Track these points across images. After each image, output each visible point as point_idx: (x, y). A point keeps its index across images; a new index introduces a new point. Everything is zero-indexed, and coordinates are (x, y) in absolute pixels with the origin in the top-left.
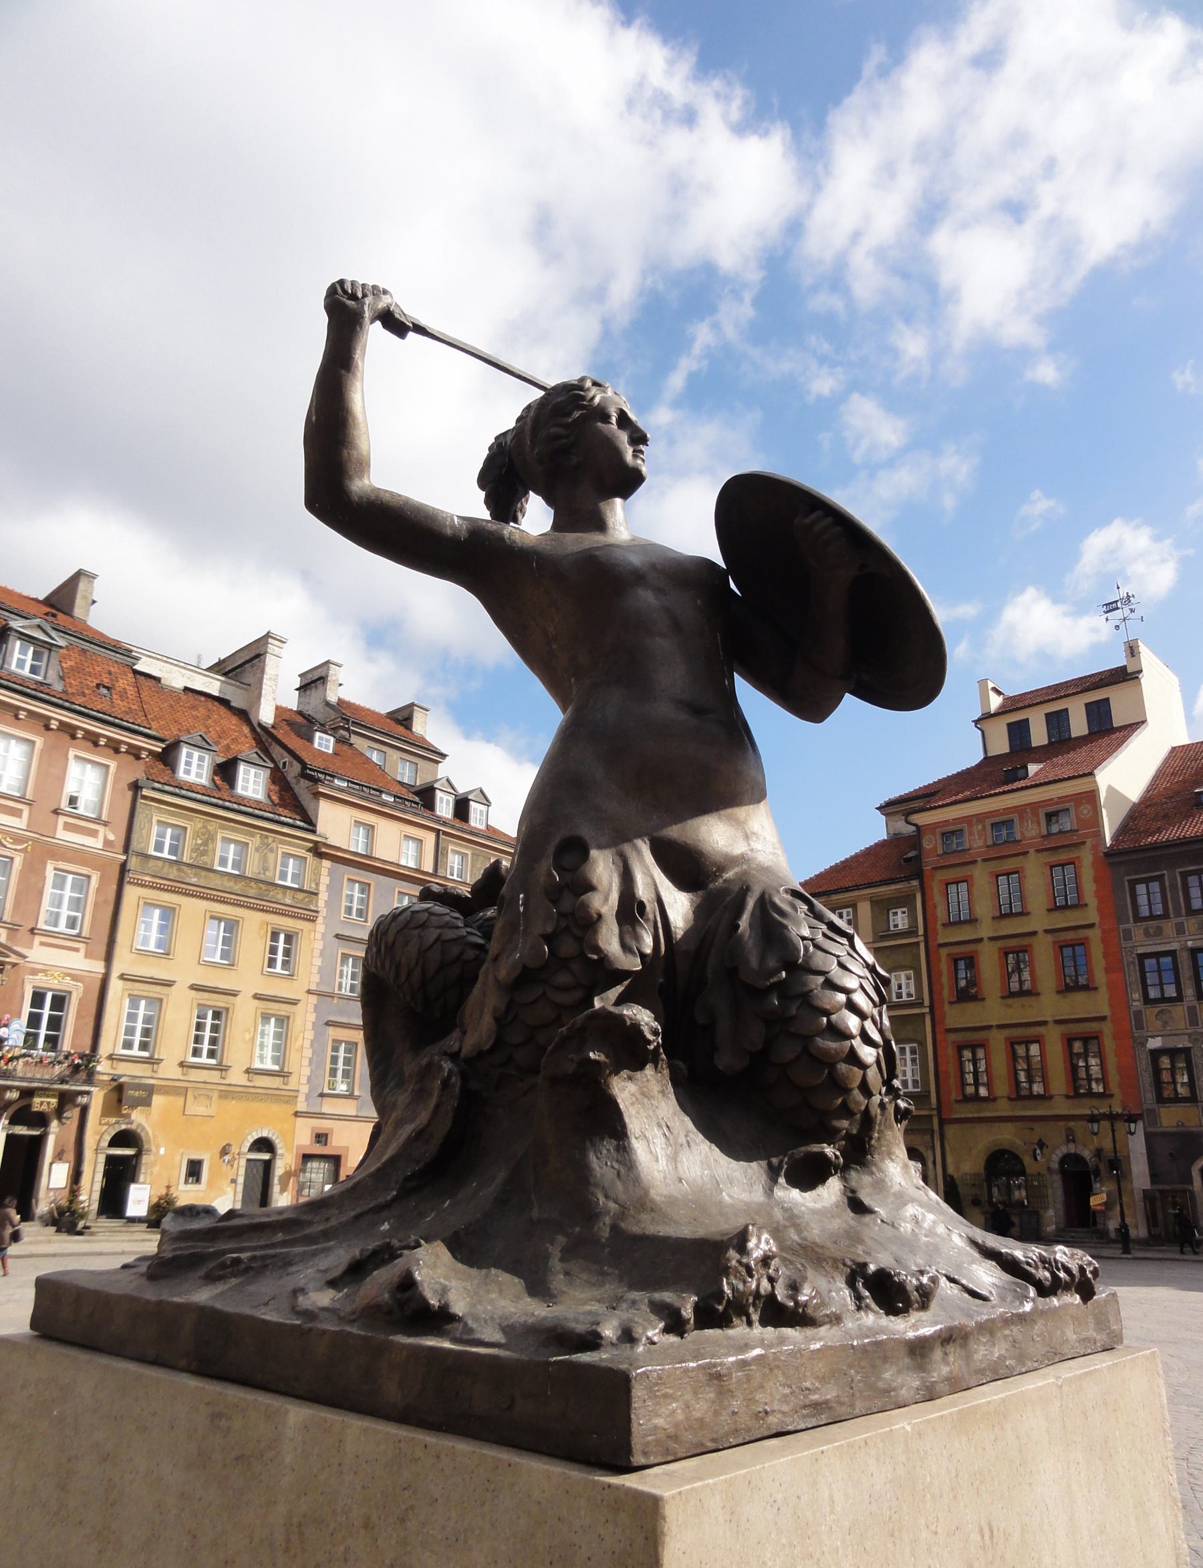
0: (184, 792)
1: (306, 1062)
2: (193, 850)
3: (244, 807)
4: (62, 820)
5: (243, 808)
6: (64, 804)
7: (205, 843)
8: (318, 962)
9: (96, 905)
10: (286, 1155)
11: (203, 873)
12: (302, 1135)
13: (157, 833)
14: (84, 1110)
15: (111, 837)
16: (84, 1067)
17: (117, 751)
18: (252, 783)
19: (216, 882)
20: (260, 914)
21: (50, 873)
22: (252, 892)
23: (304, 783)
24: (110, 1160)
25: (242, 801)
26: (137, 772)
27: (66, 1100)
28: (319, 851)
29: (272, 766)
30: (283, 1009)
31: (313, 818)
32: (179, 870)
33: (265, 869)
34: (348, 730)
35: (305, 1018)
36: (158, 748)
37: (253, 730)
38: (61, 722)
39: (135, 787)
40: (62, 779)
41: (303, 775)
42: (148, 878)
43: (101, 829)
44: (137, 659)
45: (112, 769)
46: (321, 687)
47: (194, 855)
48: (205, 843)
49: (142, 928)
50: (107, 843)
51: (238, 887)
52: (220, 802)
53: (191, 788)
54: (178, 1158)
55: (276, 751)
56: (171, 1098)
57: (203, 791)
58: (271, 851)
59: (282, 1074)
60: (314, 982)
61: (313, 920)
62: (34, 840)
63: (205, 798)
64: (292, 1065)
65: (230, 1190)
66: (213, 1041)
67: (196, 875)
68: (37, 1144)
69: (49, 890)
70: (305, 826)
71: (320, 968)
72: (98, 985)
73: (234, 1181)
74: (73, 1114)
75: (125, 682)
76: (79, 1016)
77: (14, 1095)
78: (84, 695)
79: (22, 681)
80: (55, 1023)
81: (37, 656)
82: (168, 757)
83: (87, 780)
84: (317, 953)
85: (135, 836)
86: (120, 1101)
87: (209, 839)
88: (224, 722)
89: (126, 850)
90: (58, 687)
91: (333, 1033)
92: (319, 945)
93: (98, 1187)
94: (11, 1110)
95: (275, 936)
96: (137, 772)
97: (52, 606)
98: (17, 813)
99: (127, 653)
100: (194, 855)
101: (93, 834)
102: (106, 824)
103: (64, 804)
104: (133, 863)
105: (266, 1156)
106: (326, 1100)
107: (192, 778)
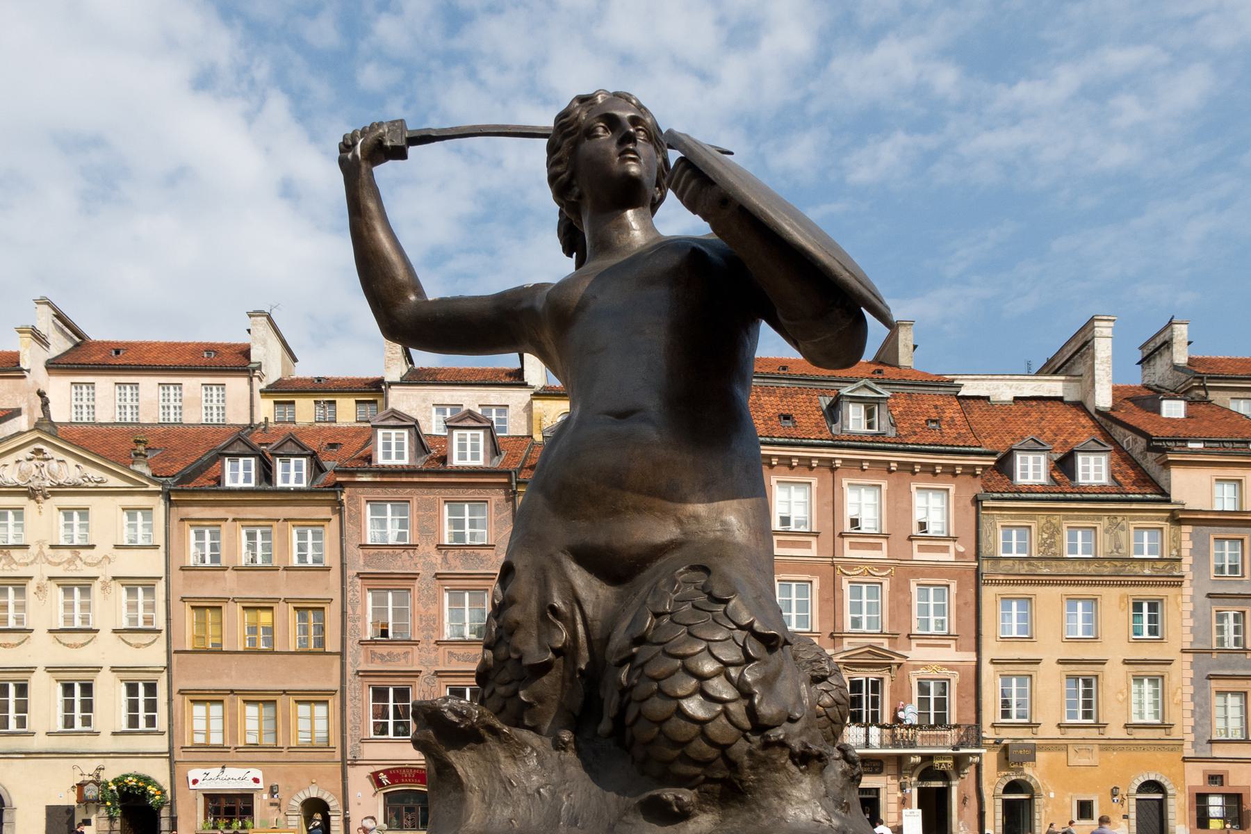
0: (1023, 495)
1: (1188, 714)
2: (1040, 545)
3: (1094, 498)
4: (915, 544)
5: (1085, 496)
6: (915, 531)
7: (1052, 536)
8: (1190, 622)
9: (958, 607)
10: (1178, 795)
11: (1054, 563)
12: (1195, 777)
13: (1009, 538)
14: (978, 767)
15: (961, 549)
16: (973, 733)
17: (955, 475)
18: (1094, 470)
19: (1068, 568)
20: (1117, 589)
21: (914, 588)
22: (1106, 571)
23: (1151, 456)
24: (1006, 802)
25: (1083, 490)
26: (977, 487)
27: (960, 762)
28: (1177, 519)
29: (1111, 447)
30: (1156, 670)
31: (1166, 488)
32: (1029, 565)
33: (1118, 547)
34: (1204, 388)
35: (1182, 675)
36: (990, 461)
37: (1092, 418)
38: (898, 462)
39: (977, 501)
40: (909, 511)
41: (1150, 449)
42: (1001, 577)
43: (951, 544)
44: (960, 386)
45: (952, 491)
46: (1166, 354)
47: (1042, 549)
48: (1052, 536)
49: (1002, 620)
50: (958, 554)
51: (1091, 569)
52: (1061, 496)
53: (1030, 489)
54: (1067, 800)
55: (1118, 432)
56: (1053, 754)
57: (1043, 489)
58: (1123, 529)
59: (1164, 726)
60: (1187, 641)
61: (1179, 584)
62: (897, 566)
63: (1044, 496)
64: (1173, 717)
65: (1123, 823)
66: (1087, 704)
67: (1046, 566)
68: (944, 794)
69: (915, 603)
70: (1159, 497)
71: (1192, 629)
72: (972, 670)
73: (1126, 817)
74: (970, 771)
75: (952, 411)
76: (959, 696)
77: (918, 759)
78: (915, 433)
79: (861, 437)
80: (941, 704)
81: (870, 414)
82: (1004, 465)
83: (932, 507)
84: (1187, 615)
85: (983, 544)
86: (1007, 758)
87: (1056, 531)
88: (1060, 420)
89: (977, 559)
90: (892, 433)
91: (1214, 685)
92: (1190, 607)
93: (999, 823)
94: (918, 771)
95: (1137, 607)
96: (977, 487)
97: (881, 363)
98: (877, 547)
99: (950, 384)
100: (1042, 549)
101: (945, 549)
102: (955, 539)
103: (915, 531)
104: (986, 566)
105: (1159, 796)
106: (1215, 746)
107: (1030, 480)
